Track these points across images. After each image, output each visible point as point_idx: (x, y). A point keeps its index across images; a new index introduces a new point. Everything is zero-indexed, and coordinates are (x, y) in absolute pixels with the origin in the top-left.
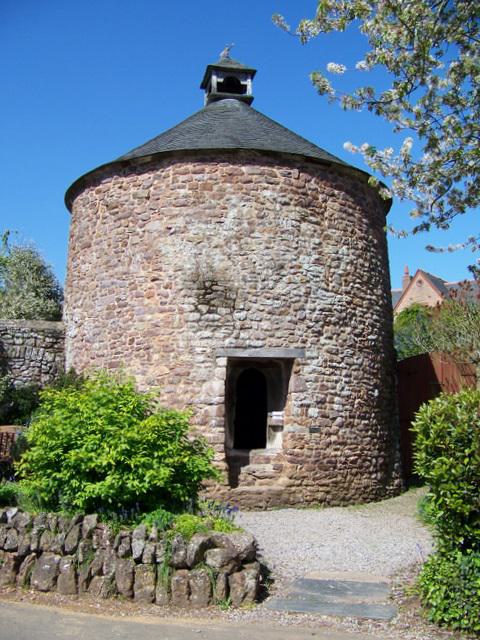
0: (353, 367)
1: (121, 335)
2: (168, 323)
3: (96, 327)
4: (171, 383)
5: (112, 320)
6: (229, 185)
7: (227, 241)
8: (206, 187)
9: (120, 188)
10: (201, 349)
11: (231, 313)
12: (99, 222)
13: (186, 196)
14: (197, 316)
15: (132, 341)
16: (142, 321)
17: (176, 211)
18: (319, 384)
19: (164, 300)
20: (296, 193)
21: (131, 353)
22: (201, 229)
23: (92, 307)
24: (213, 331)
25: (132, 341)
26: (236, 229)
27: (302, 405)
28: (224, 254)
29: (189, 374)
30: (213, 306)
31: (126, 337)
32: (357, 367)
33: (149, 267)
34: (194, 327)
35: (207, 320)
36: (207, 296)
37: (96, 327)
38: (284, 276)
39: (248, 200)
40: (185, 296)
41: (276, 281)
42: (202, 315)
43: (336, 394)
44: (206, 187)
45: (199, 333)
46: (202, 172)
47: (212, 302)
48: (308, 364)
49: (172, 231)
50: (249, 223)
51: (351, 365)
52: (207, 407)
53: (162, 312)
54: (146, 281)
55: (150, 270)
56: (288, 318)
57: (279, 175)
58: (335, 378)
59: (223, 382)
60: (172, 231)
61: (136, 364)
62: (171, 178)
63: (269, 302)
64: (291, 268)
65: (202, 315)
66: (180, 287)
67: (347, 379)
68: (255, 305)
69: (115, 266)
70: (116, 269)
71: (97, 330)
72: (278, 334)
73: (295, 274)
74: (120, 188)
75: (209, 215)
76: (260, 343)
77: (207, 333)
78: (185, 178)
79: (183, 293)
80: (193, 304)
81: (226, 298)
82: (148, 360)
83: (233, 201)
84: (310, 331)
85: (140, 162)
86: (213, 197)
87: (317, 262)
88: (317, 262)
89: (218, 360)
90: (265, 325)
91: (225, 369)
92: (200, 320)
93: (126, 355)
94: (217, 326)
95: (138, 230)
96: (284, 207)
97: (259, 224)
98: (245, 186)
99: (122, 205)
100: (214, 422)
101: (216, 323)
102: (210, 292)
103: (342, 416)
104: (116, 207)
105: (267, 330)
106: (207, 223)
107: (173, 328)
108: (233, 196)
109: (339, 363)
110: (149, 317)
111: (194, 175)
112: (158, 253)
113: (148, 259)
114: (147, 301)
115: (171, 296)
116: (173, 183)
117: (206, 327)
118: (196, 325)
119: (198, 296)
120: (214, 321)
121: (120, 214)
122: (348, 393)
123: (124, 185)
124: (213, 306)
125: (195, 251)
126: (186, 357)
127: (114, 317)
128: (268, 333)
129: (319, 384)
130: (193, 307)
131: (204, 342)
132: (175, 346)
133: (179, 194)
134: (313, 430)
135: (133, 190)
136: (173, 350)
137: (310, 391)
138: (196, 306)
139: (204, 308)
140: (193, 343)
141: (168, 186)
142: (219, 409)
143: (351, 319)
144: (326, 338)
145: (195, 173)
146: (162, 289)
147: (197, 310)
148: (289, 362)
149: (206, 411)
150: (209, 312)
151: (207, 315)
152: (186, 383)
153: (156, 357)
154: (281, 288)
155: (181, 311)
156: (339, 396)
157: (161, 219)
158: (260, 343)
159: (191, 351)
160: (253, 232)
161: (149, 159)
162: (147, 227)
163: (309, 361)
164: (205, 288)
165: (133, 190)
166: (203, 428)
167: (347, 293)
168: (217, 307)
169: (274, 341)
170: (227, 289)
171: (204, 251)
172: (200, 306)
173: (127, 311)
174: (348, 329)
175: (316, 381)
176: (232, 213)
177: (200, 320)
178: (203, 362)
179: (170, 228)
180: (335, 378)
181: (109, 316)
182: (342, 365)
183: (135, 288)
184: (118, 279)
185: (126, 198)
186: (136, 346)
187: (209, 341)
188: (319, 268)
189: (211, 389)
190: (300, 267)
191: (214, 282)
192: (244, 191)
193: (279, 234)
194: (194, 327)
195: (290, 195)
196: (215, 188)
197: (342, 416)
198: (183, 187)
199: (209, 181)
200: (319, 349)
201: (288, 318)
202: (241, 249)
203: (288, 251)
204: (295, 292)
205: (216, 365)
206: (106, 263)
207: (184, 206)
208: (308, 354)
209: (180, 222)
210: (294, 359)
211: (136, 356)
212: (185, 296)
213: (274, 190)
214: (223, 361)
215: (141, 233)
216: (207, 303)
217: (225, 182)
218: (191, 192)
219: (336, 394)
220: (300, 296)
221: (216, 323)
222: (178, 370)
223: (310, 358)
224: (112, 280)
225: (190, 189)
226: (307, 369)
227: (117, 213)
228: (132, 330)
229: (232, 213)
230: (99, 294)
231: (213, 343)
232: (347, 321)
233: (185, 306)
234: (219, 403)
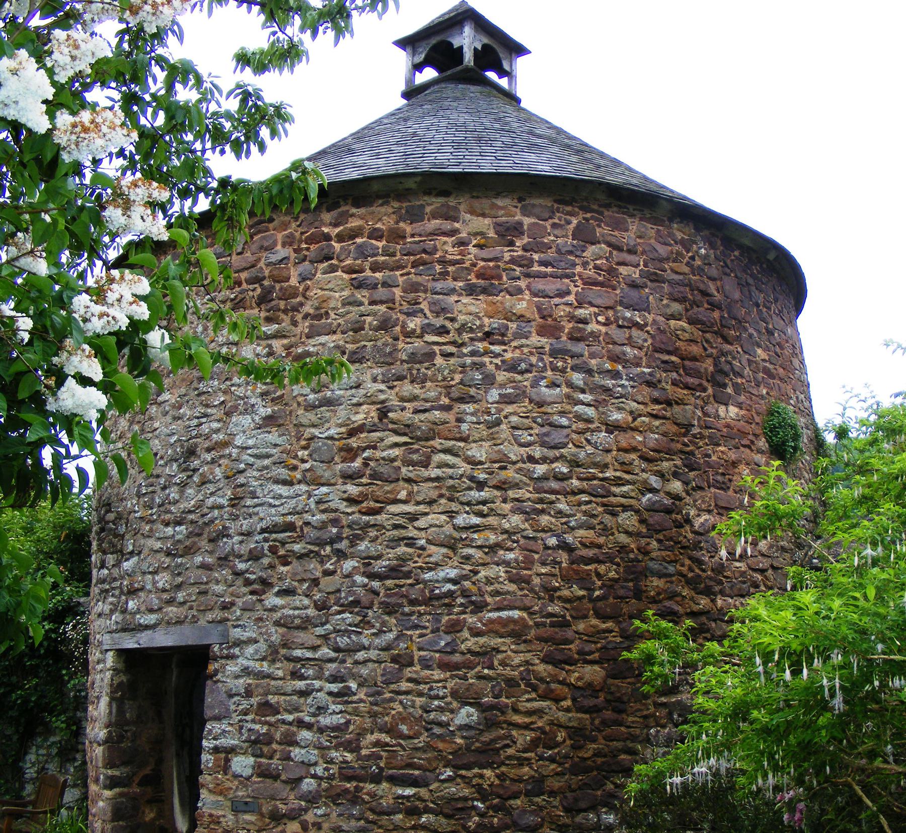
0: (361, 655)
18: (254, 701)
32: (373, 654)
38: (195, 470)
41: (183, 485)
43: (301, 724)
48: (232, 657)
51: (351, 650)
56: (198, 559)
58: (301, 684)
63: (169, 531)
64: (209, 450)
67: (334, 687)
72: (180, 596)
73: (213, 461)
76: (151, 619)
84: (239, 582)
87: (270, 421)
88: (270, 421)
90: (163, 579)
103: (314, 776)
105: (164, 590)
109: (314, 648)
122: (339, 719)
128: (165, 596)
129: (254, 701)
134: (238, 807)
137: (236, 718)
143: (354, 540)
144: (279, 594)
156: (309, 726)
158: (151, 619)
163: (237, 651)
167: (348, 477)
169: (172, 611)
174: (349, 565)
175: (249, 693)
180: (301, 684)
182: (325, 652)
188: (273, 437)
190: (225, 444)
197: (314, 776)
200: (260, 619)
201: (198, 559)
203: (205, 415)
204: (210, 501)
208: (236, 633)
210: (208, 647)
219: (301, 724)
220: (221, 507)
223: (238, 643)
226: (232, 668)
232: (343, 545)
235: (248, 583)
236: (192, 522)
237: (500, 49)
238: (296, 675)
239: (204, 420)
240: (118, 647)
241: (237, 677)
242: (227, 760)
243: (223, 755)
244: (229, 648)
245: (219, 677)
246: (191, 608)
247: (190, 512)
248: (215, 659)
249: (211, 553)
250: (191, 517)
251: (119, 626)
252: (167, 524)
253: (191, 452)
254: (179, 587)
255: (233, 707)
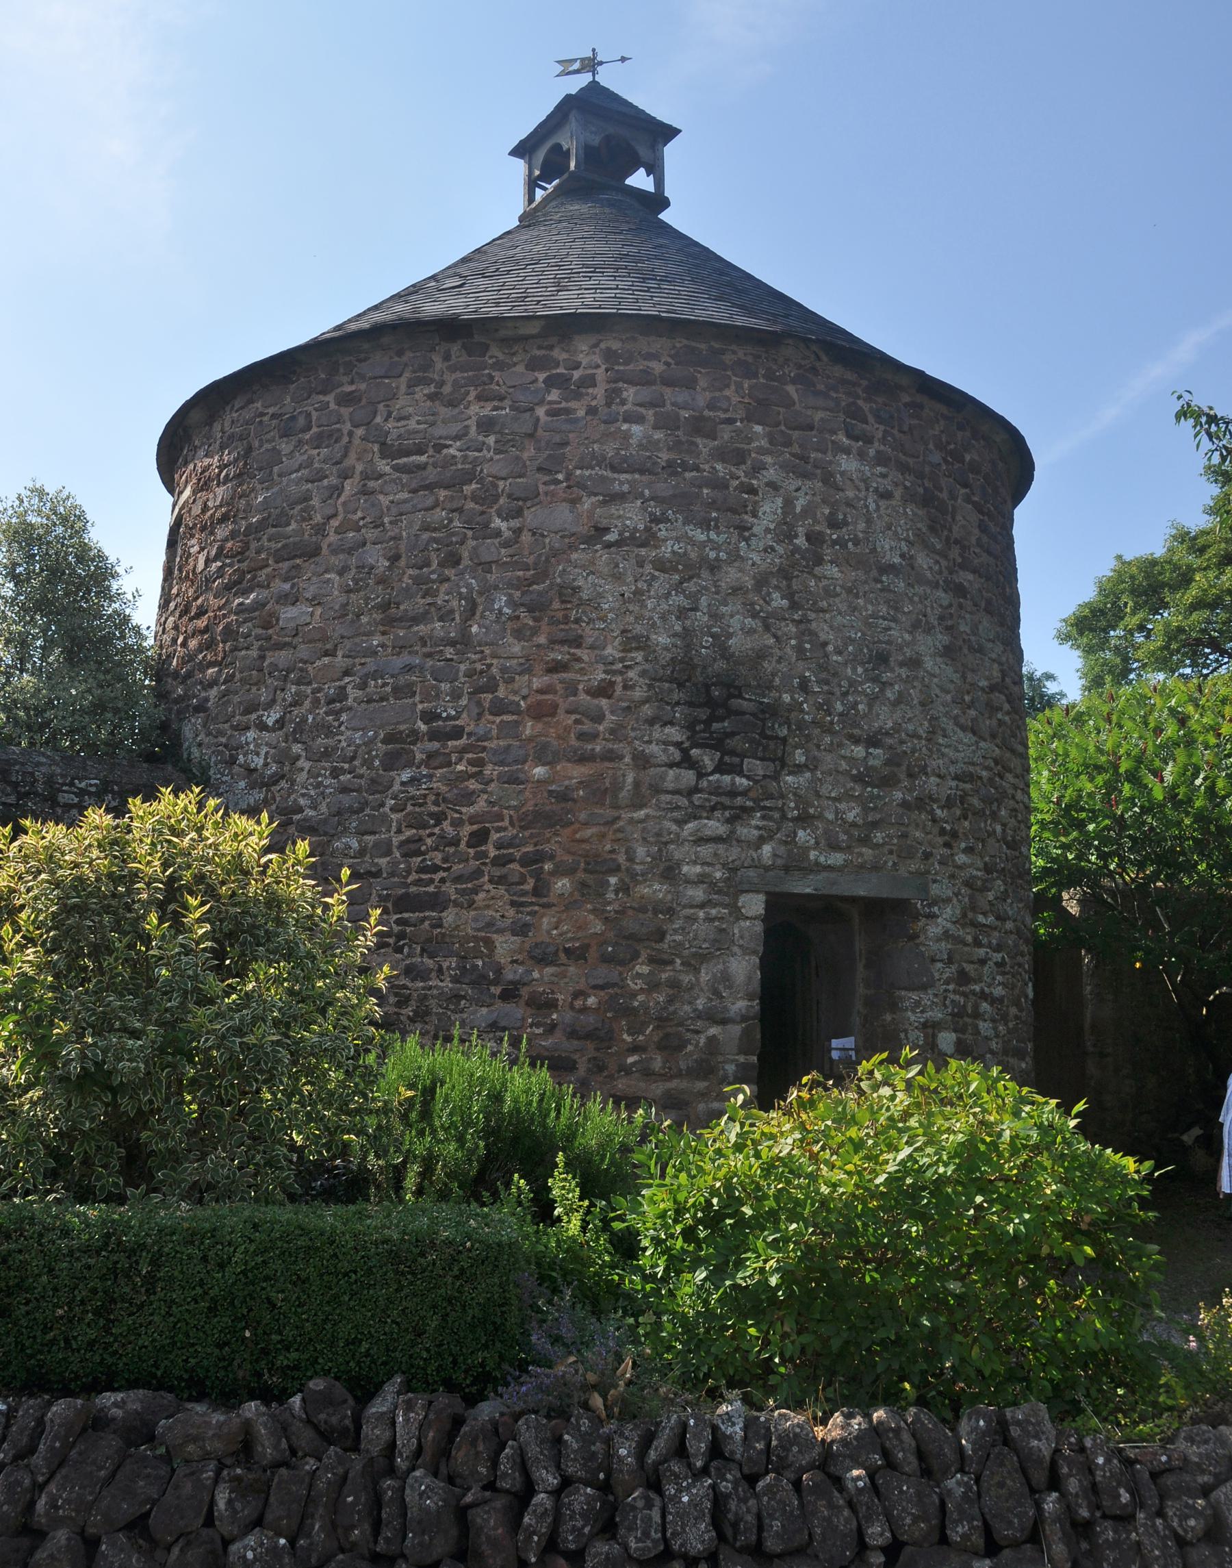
1: (439, 818)
2: (601, 793)
3: (345, 790)
4: (607, 959)
5: (406, 775)
6: (758, 429)
7: (761, 582)
8: (700, 426)
9: (432, 397)
10: (698, 869)
11: (776, 777)
12: (349, 487)
13: (649, 444)
14: (689, 777)
15: (479, 838)
16: (513, 780)
17: (622, 482)
19: (587, 726)
20: (904, 468)
21: (478, 873)
22: (691, 541)
23: (329, 731)
24: (729, 821)
25: (479, 838)
26: (780, 549)
27: (925, 1025)
28: (754, 615)
29: (661, 935)
30: (733, 753)
31: (457, 824)
33: (535, 632)
34: (678, 808)
35: (716, 790)
36: (715, 726)
37: (345, 790)
39: (805, 476)
40: (651, 722)
41: (873, 700)
42: (700, 776)
44: (700, 426)
45: (690, 826)
46: (690, 384)
47: (731, 743)
49: (612, 537)
50: (808, 538)
52: (713, 1031)
53: (583, 759)
54: (529, 671)
55: (542, 640)
57: (871, 419)
59: (756, 960)
60: (612, 537)
61: (494, 902)
62: (599, 391)
63: (859, 751)
65: (700, 776)
66: (638, 694)
68: (828, 758)
69: (416, 620)
70: (421, 629)
71: (347, 800)
72: (879, 837)
74: (432, 397)
75: (712, 505)
76: (837, 859)
77: (714, 826)
78: (646, 393)
79: (647, 711)
80: (678, 745)
81: (763, 735)
82: (536, 892)
83: (771, 474)
85: (503, 333)
86: (721, 455)
89: (743, 899)
90: (853, 814)
91: (759, 927)
92: (696, 790)
93: (458, 879)
94: (744, 809)
95: (497, 523)
96: (882, 503)
97: (835, 542)
98: (796, 434)
99: (439, 448)
100: (731, 1068)
101: (739, 801)
102: (723, 712)
104: (421, 452)
105: (854, 825)
106: (705, 525)
107: (616, 807)
108: (769, 459)
110: (539, 771)
111: (668, 392)
112: (568, 593)
113: (537, 608)
114: (529, 728)
115: (610, 717)
116: (608, 405)
117: (713, 809)
118: (683, 802)
119: (690, 726)
120: (733, 793)
121: (431, 475)
123: (447, 389)
124: (733, 753)
125: (678, 600)
126: (656, 890)
127: (410, 764)
130: (677, 755)
131: (706, 851)
132: (621, 859)
133: (627, 436)
135: (477, 410)
136: (616, 869)
138: (685, 752)
139: (708, 760)
140: (678, 853)
141: (592, 411)
142: (746, 1033)
145: (668, 382)
146: (583, 696)
147: (687, 761)
148: (900, 907)
149: (712, 1040)
150: (720, 768)
151: (717, 776)
152: (651, 961)
153: (562, 885)
154: (885, 718)
155: (642, 761)
157: (574, 502)
158: (837, 859)
159: (670, 873)
160: (819, 561)
161: (533, 329)
162: (532, 517)
164: (710, 703)
165: (477, 410)
166: (701, 1085)
168: (743, 756)
170: (772, 711)
171: (704, 601)
172: (694, 752)
173: (463, 750)
176: (770, 510)
177: (696, 790)
178: (702, 906)
179: (606, 530)
181: (392, 762)
183: (491, 687)
184: (429, 655)
185: (455, 428)
186: (493, 853)
187: (721, 848)
189: (726, 978)
191: (733, 689)
192: (796, 449)
193: (874, 573)
194: (678, 808)
195: (894, 475)
196: (726, 433)
198: (640, 419)
199: (706, 413)
202: (794, 606)
203: (894, 620)
205: (737, 914)
206: (385, 606)
207: (642, 472)
208: (935, 890)
209: (632, 516)
211: (497, 881)
212: (651, 722)
213: (862, 455)
214: (754, 904)
215: (507, 534)
216: (717, 744)
217: (749, 419)
218: (659, 435)
221: (739, 801)
222: (630, 924)
224: (406, 659)
225: (655, 427)
226: (934, 930)
227: (423, 467)
228: (481, 805)
229: (770, 510)
230: (353, 693)
231: (734, 853)
233: (654, 748)
234: (744, 1018)
235: (943, 832)
236: (891, 747)
237: (646, 137)
238: (977, 943)
239: (893, 625)
240: (772, 889)
241: (939, 940)
242: (934, 1036)
243: (930, 1031)
244: (929, 906)
245: (922, 938)
246: (891, 852)
247: (887, 734)
248: (916, 916)
249: (910, 790)
250: (890, 741)
251: (779, 862)
252: (857, 741)
253: (882, 659)
254: (875, 825)
255: (937, 976)
